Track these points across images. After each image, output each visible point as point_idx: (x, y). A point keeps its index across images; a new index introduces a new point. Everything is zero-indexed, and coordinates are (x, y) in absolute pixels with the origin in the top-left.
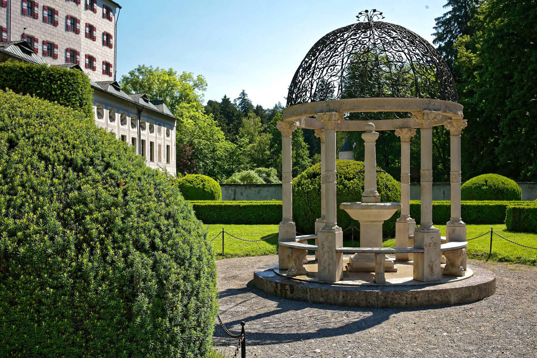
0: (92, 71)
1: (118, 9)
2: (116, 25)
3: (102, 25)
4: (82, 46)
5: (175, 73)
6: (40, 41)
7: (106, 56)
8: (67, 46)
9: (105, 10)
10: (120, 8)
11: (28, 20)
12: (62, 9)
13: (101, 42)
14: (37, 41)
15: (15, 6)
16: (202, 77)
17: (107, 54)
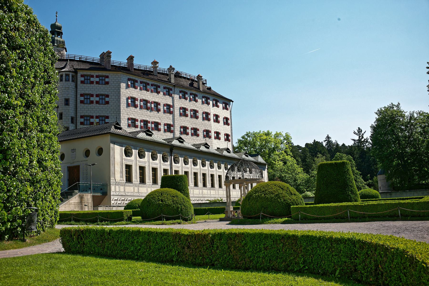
0: (218, 140)
1: (231, 103)
2: (231, 112)
3: (223, 113)
4: (212, 127)
5: (271, 133)
6: (190, 128)
7: (226, 131)
8: (204, 129)
9: (224, 105)
10: (233, 102)
11: (183, 118)
12: (200, 109)
13: (223, 123)
14: (188, 128)
15: (177, 112)
16: (288, 134)
17: (227, 129)
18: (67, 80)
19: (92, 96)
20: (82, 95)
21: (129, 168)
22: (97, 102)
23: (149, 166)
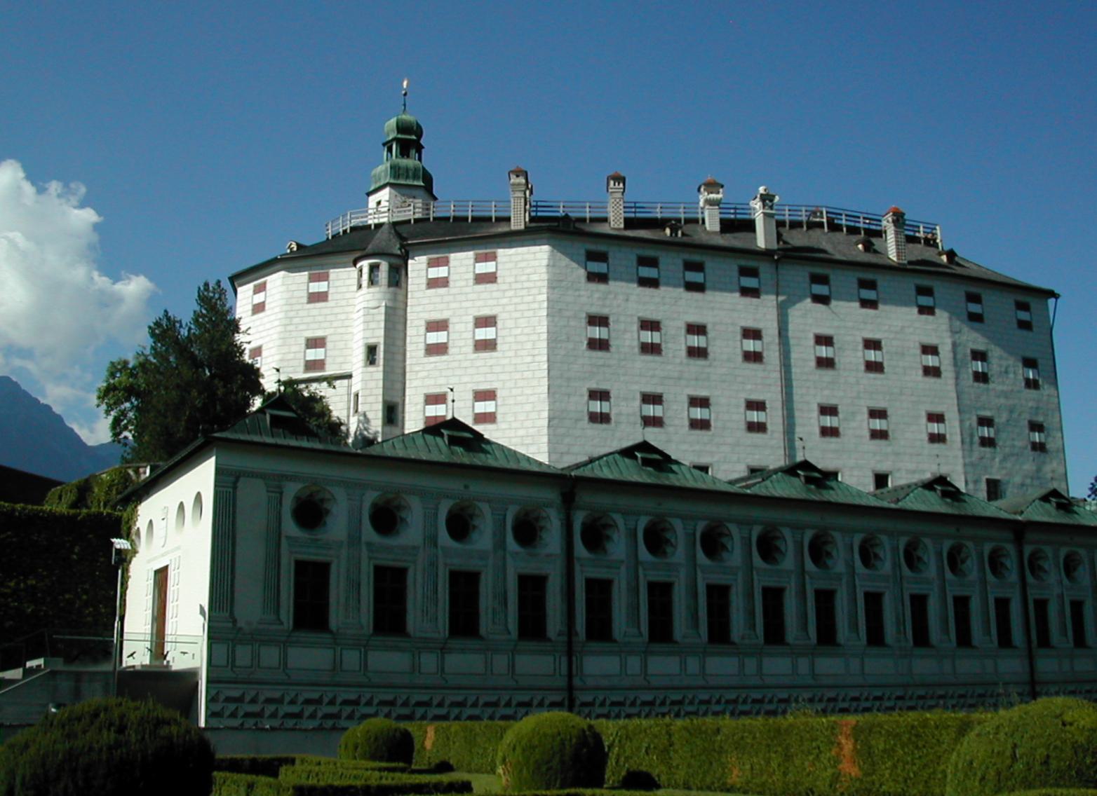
1: (1051, 301)
23: (433, 564)
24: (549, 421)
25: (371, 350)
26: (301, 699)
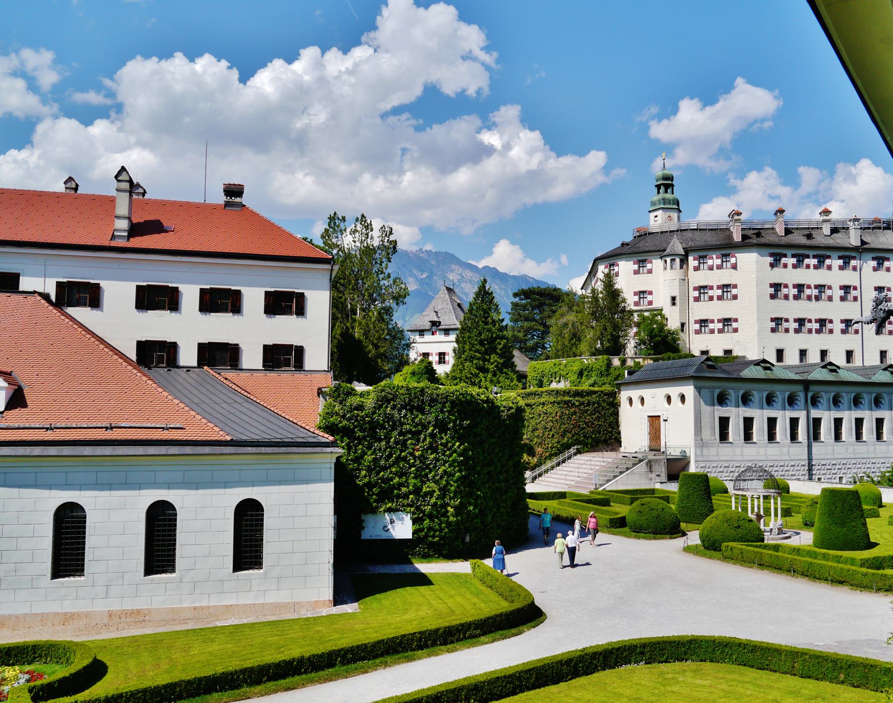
18: (674, 267)
19: (711, 288)
20: (695, 289)
21: (724, 422)
22: (720, 298)
24: (758, 332)
25: (674, 299)
26: (723, 466)
